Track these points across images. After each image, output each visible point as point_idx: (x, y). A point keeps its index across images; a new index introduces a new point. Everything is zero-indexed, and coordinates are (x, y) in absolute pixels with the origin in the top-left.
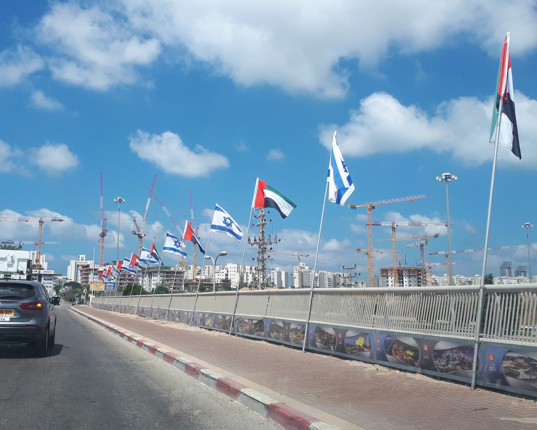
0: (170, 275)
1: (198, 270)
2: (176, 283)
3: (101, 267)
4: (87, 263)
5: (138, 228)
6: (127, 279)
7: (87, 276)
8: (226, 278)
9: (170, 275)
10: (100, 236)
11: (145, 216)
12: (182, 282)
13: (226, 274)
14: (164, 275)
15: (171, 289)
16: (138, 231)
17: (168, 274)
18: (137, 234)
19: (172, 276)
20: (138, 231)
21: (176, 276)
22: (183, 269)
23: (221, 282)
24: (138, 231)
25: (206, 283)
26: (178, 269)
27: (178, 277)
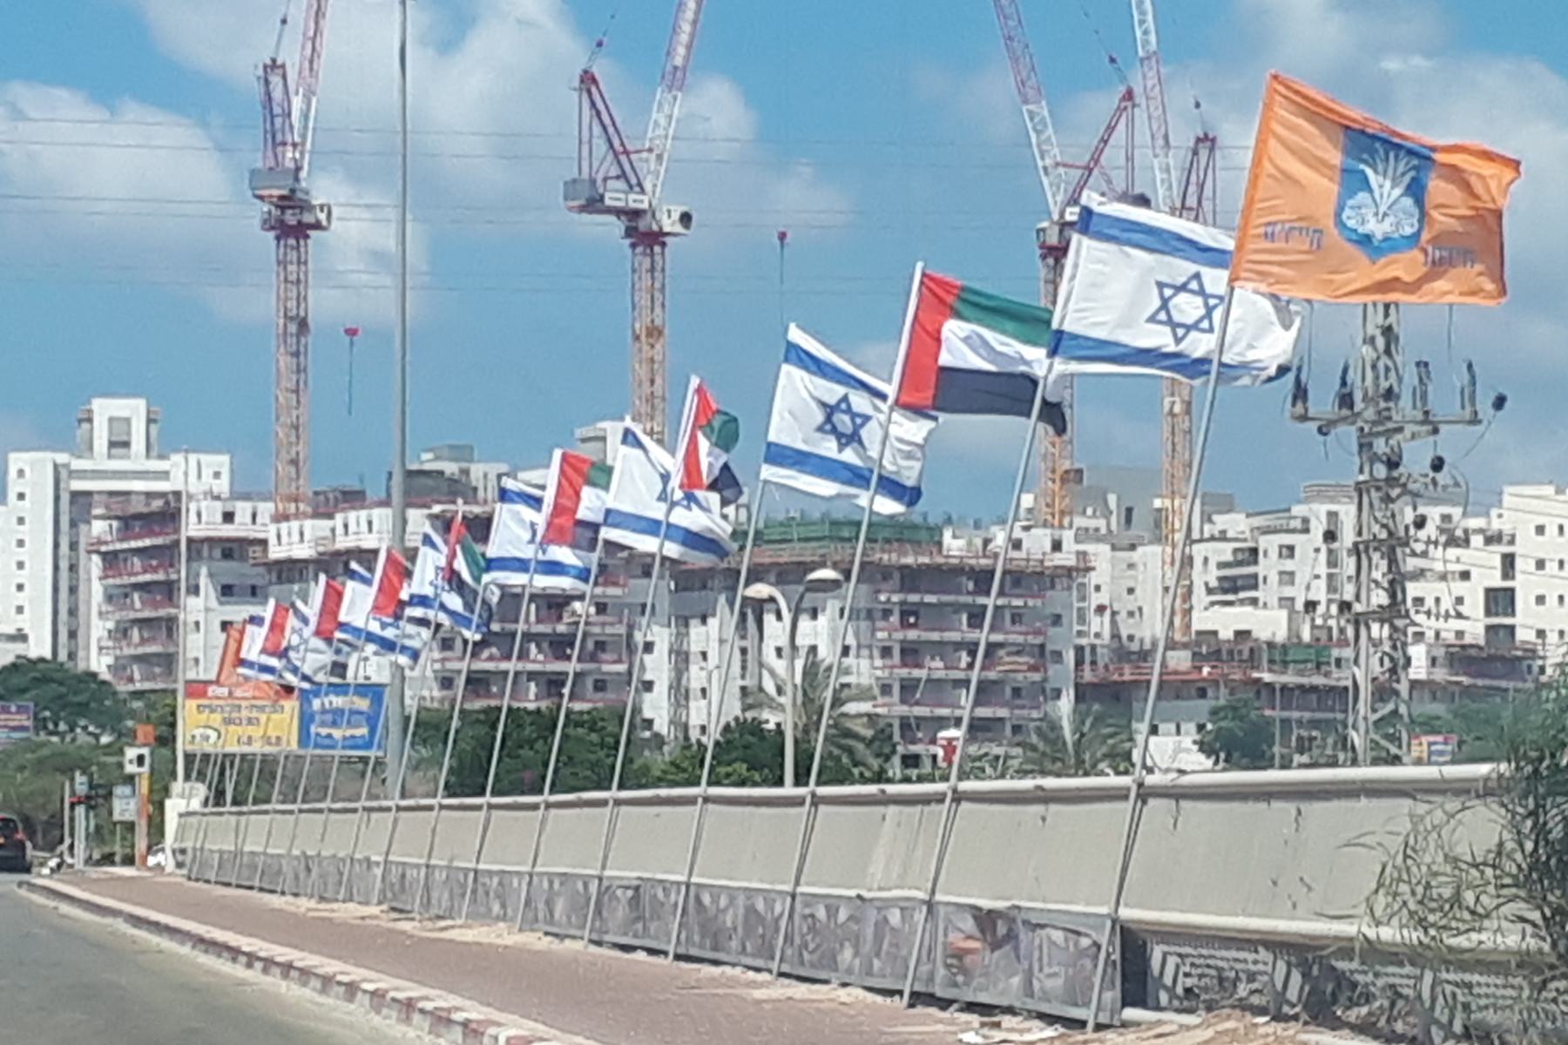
0: (930, 599)
1: (1225, 551)
2: (992, 675)
3: (295, 525)
4: (165, 475)
5: (620, 153)
6: (528, 637)
7: (162, 612)
8: (1489, 628)
9: (930, 599)
10: (271, 235)
11: (684, 38)
12: (1053, 670)
13: (1491, 593)
14: (883, 598)
15: (952, 733)
16: (621, 185)
17: (914, 590)
18: (618, 212)
19: (957, 608)
20: (623, 176)
21: (997, 608)
22: (1057, 546)
23: (1441, 675)
24: (623, 176)
25: (1290, 678)
26: (1017, 545)
27: (1016, 618)
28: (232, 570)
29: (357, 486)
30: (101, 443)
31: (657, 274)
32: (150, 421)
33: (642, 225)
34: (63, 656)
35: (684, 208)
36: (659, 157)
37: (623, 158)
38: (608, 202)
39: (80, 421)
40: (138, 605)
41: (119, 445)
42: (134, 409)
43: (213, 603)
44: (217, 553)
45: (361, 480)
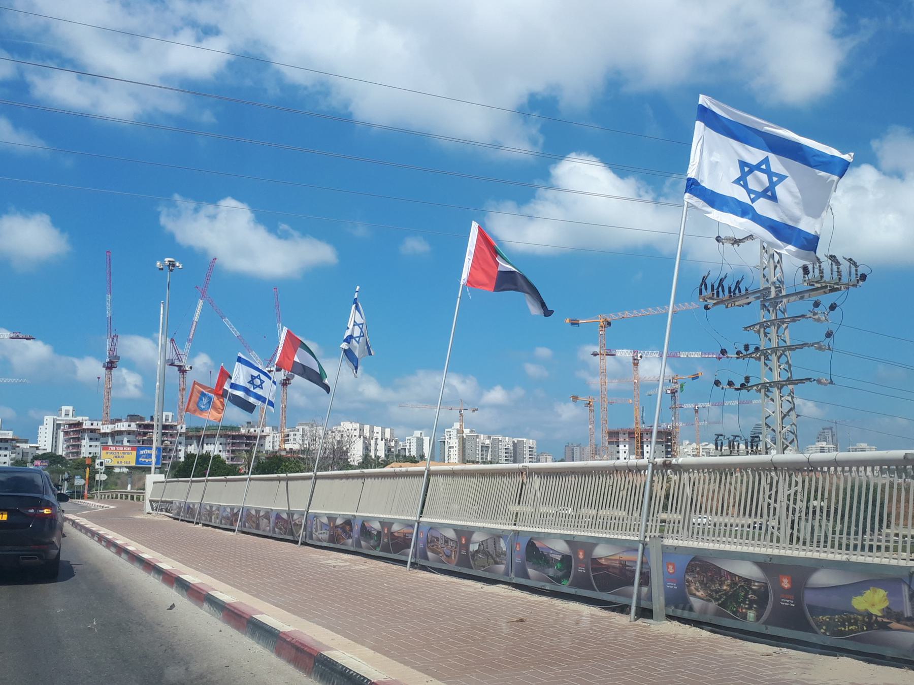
0: (238, 441)
3: (106, 426)
7: (77, 443)
9: (238, 441)
10: (105, 368)
11: (192, 333)
16: (178, 361)
17: (234, 439)
18: (177, 366)
19: (243, 443)
20: (178, 359)
28: (92, 435)
29: (120, 418)
30: (63, 414)
31: (185, 379)
32: (73, 411)
33: (182, 369)
34: (53, 451)
35: (191, 366)
36: (186, 356)
37: (179, 356)
38: (175, 364)
39: (59, 410)
40: (72, 442)
41: (67, 415)
42: (70, 408)
43: (88, 441)
44: (89, 431)
45: (121, 417)
